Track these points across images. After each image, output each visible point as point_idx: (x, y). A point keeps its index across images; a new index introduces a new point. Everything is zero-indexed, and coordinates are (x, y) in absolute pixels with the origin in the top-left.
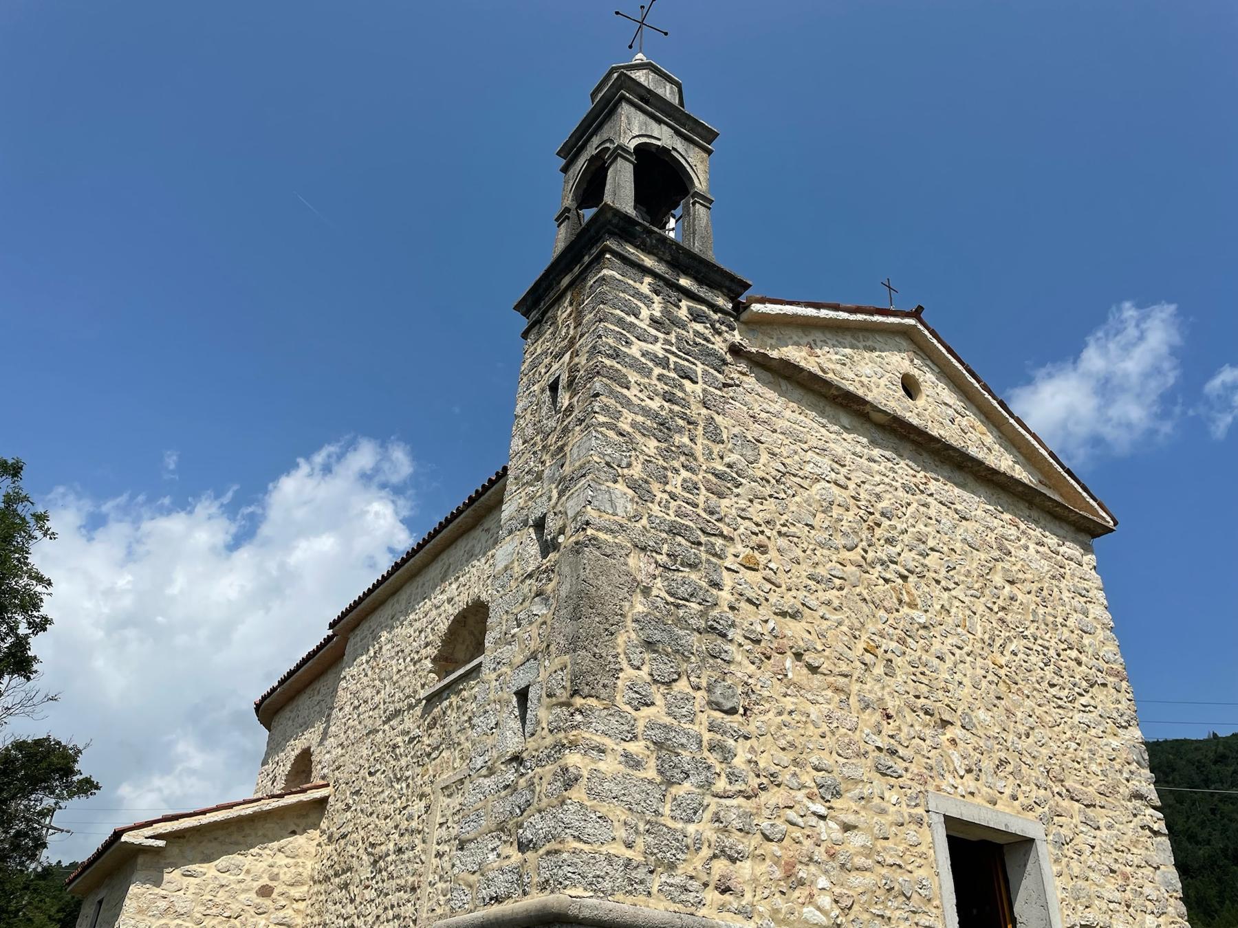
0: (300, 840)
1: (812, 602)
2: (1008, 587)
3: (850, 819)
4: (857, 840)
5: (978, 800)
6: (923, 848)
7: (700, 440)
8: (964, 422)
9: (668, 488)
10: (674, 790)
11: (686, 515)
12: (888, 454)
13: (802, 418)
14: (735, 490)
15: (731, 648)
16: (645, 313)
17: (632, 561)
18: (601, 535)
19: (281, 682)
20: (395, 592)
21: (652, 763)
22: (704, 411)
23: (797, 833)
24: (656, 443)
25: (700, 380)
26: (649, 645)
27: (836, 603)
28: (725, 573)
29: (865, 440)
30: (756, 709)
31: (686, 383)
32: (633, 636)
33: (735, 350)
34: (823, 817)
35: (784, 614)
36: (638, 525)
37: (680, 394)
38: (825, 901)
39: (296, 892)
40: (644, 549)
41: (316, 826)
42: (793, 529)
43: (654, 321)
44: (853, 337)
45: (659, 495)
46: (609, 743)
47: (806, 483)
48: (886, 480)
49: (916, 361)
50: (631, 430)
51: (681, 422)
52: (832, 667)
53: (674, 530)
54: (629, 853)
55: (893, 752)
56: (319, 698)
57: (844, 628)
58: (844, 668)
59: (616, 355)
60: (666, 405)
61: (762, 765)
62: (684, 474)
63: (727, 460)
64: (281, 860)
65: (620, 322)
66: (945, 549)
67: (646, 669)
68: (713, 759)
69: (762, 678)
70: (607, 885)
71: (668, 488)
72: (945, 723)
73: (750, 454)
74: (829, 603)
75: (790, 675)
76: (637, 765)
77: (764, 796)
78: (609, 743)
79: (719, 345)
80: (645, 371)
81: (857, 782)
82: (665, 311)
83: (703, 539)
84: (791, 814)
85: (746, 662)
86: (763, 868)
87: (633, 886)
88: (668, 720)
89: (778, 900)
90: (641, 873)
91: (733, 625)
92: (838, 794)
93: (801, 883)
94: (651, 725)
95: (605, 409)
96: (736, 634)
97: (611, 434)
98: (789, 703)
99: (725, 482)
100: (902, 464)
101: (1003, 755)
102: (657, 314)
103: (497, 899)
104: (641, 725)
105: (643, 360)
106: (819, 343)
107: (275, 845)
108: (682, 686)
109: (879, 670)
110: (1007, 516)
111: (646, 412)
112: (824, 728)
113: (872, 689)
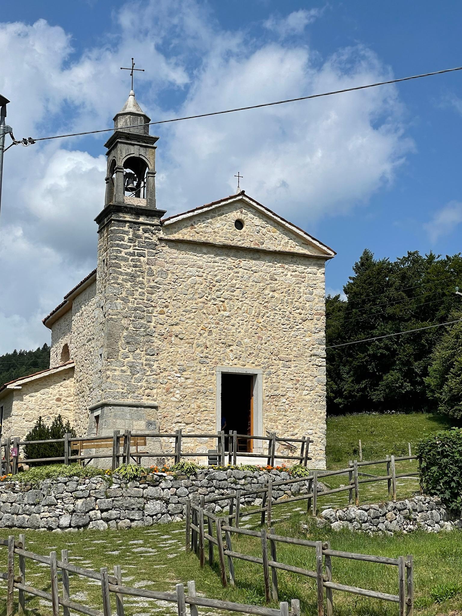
0: (67, 382)
1: (183, 318)
2: (271, 293)
3: (188, 376)
4: (189, 381)
5: (238, 366)
6: (212, 381)
7: (145, 277)
8: (264, 230)
9: (134, 297)
10: (135, 376)
11: (140, 304)
12: (222, 258)
13: (187, 255)
14: (158, 290)
15: (154, 338)
16: (126, 238)
17: (122, 322)
18: (113, 317)
19: (51, 314)
20: (85, 289)
21: (129, 371)
22: (148, 266)
23: (171, 382)
24: (130, 283)
25: (146, 255)
26: (128, 343)
27: (192, 317)
28: (153, 317)
29: (212, 256)
30: (161, 353)
31: (142, 258)
32: (123, 341)
33: (160, 240)
34: (180, 377)
35: (173, 325)
36: (125, 311)
37: (139, 264)
38: (178, 396)
39: (69, 399)
40: (126, 317)
41: (72, 377)
42: (179, 297)
43: (130, 240)
44: (213, 213)
45: (131, 300)
46: (117, 368)
47: (185, 280)
48: (220, 268)
49: (244, 211)
50: (121, 282)
51: (139, 273)
52: (188, 337)
53: (136, 309)
54: (123, 391)
55: (206, 357)
56: (67, 323)
57: (194, 325)
58: (192, 336)
59: (117, 258)
60: (134, 269)
61: (161, 367)
62: (140, 290)
63: (155, 281)
64: (62, 389)
65: (118, 245)
66: (243, 286)
67: (127, 349)
68: (146, 368)
69: (165, 345)
70: (117, 397)
71: (134, 297)
72: (230, 346)
73: (164, 276)
74: (190, 318)
75: (173, 342)
76: (125, 372)
77: (161, 374)
78: (117, 368)
79: (154, 239)
80: (126, 260)
81: (191, 367)
82: (134, 234)
83: (145, 309)
84: (169, 377)
85: (158, 341)
86: (159, 391)
87: (123, 397)
88: (133, 360)
89: (164, 397)
90: (126, 394)
91: (155, 332)
92: (185, 371)
93: (171, 392)
94: (128, 362)
95: (113, 278)
96: (156, 335)
97: (116, 285)
98: (172, 350)
99: (153, 290)
100: (229, 259)
101: (251, 352)
102: (131, 236)
103: (99, 401)
104: (125, 363)
105: (126, 256)
106: (196, 222)
107: (59, 384)
108: (138, 351)
109: (206, 334)
110: (279, 265)
111: (127, 274)
112: (183, 354)
113: (202, 340)
